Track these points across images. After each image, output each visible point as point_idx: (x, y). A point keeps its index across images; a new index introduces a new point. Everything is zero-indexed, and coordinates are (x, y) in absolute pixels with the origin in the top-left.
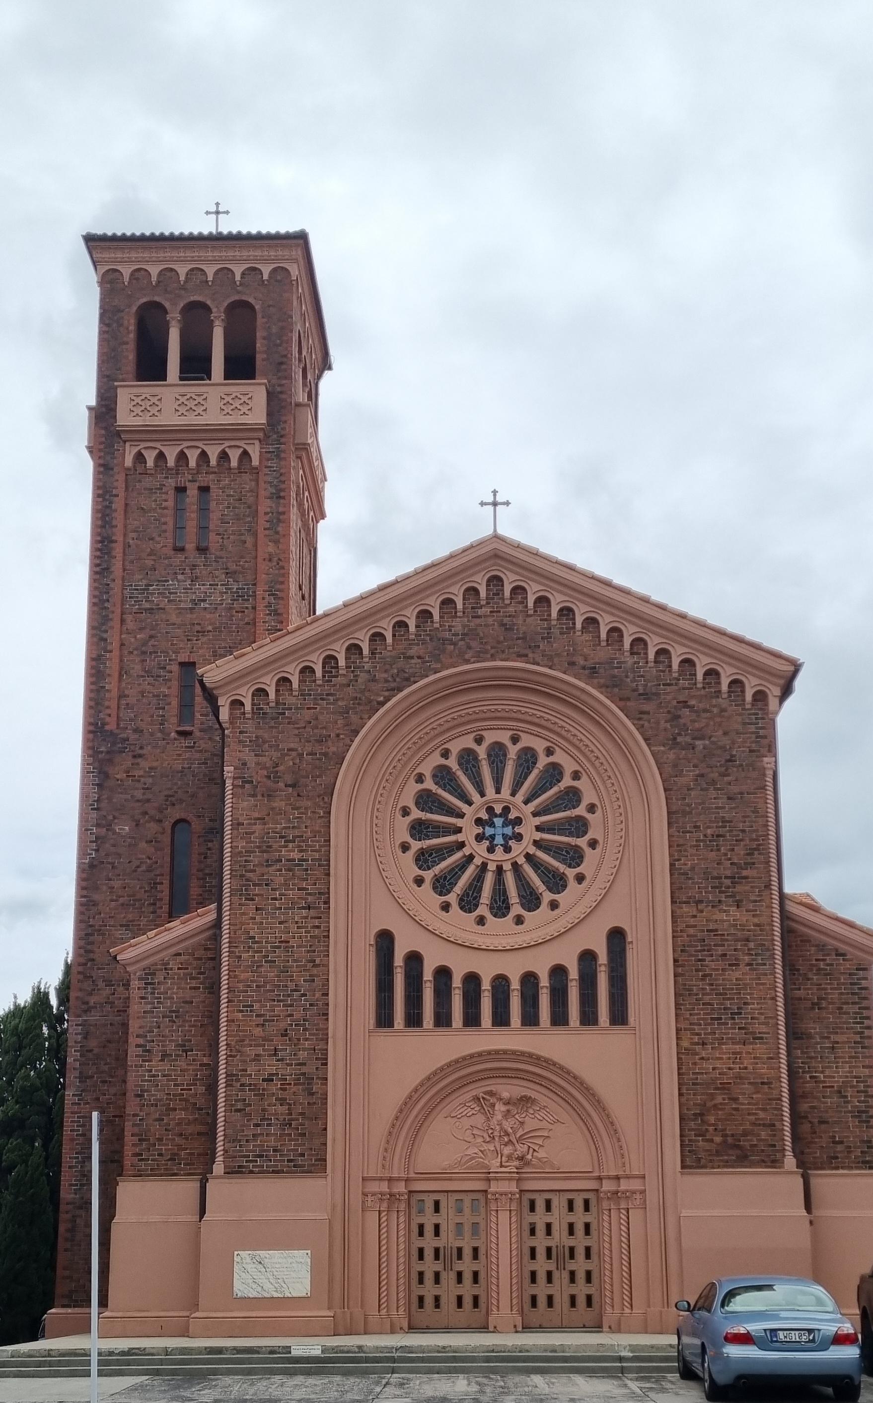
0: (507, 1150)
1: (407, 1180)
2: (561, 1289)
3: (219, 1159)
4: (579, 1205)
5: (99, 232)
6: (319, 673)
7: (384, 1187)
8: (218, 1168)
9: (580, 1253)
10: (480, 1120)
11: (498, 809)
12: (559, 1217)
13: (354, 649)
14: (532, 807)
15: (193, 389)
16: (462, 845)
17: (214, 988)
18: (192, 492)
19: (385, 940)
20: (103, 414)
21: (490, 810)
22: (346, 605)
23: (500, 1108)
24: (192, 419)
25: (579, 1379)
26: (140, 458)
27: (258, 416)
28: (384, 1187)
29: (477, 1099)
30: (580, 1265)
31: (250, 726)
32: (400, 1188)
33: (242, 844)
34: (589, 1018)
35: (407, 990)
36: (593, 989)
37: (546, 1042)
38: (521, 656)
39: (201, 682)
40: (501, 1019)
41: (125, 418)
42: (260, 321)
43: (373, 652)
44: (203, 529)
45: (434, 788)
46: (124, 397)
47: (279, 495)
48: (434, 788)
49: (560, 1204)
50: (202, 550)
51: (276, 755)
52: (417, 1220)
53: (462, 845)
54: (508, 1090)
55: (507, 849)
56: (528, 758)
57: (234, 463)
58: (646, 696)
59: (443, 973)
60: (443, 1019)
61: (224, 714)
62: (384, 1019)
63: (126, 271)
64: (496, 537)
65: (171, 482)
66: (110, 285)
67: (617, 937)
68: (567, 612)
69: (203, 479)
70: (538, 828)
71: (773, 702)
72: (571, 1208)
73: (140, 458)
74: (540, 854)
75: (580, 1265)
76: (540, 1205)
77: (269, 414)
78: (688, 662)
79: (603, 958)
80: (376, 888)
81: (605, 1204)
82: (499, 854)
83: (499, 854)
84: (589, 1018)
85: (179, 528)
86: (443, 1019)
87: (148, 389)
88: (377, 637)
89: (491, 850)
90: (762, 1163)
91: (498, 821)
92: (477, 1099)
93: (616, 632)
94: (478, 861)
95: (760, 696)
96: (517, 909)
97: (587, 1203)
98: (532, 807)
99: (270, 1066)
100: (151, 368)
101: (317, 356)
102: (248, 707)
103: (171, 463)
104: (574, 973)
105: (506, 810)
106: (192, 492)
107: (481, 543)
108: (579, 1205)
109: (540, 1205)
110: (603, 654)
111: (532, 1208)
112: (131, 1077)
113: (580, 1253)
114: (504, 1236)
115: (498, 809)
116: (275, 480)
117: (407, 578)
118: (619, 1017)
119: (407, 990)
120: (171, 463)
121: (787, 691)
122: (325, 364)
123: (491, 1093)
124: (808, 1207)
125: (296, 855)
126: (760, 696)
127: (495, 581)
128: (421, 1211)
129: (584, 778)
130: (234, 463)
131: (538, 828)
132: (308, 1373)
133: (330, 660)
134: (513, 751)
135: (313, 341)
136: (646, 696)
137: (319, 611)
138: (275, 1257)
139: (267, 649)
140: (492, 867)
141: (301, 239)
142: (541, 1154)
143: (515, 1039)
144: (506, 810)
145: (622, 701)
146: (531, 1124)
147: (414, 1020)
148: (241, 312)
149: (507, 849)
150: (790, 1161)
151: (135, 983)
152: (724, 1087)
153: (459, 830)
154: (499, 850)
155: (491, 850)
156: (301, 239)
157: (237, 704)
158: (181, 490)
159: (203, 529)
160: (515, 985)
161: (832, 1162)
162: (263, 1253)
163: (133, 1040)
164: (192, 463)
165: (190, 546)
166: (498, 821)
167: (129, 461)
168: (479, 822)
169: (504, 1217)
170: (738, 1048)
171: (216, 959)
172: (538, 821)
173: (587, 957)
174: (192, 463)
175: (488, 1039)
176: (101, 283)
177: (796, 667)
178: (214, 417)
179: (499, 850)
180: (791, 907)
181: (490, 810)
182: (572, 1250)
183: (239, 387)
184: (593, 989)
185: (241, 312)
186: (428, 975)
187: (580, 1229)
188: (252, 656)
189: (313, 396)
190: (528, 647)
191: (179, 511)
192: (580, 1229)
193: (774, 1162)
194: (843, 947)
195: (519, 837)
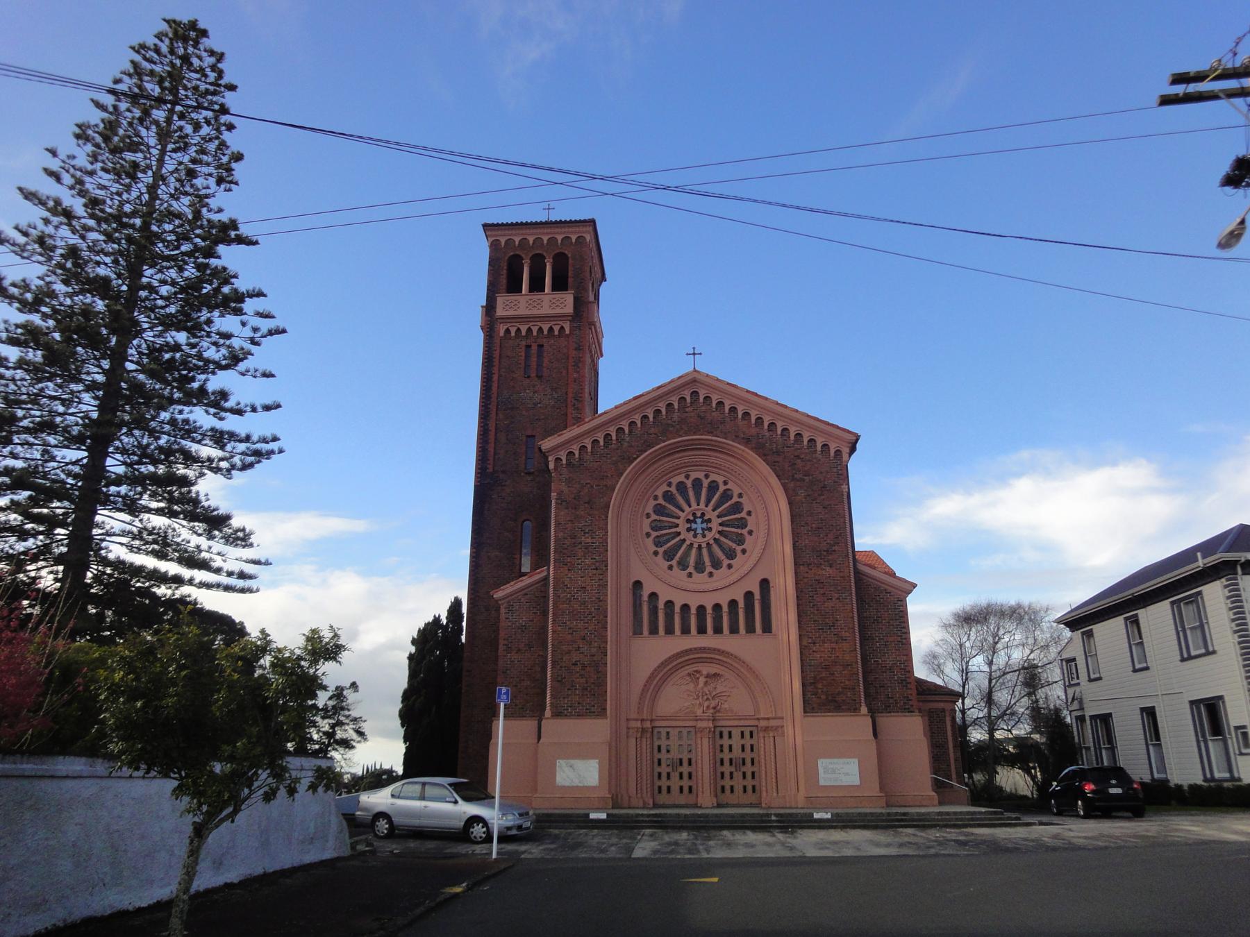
0: (706, 704)
1: (652, 720)
2: (738, 782)
3: (548, 708)
4: (747, 734)
5: (490, 222)
6: (602, 443)
7: (639, 724)
8: (548, 713)
9: (748, 761)
10: (691, 686)
11: (699, 514)
12: (736, 742)
13: (620, 430)
14: (716, 513)
15: (536, 296)
16: (679, 534)
17: (545, 613)
18: (534, 347)
19: (638, 585)
20: (490, 309)
21: (694, 514)
22: (616, 407)
23: (702, 680)
24: (535, 312)
25: (749, 833)
26: (508, 331)
27: (569, 309)
28: (639, 724)
29: (689, 675)
30: (748, 769)
31: (565, 471)
32: (648, 725)
33: (561, 535)
34: (750, 629)
35: (652, 615)
36: (753, 611)
37: (726, 642)
38: (710, 433)
39: (540, 449)
40: (702, 630)
41: (500, 312)
42: (570, 261)
43: (630, 431)
44: (539, 365)
45: (664, 503)
46: (501, 300)
47: (579, 349)
48: (664, 503)
49: (736, 733)
50: (539, 377)
51: (578, 486)
52: (656, 743)
53: (679, 534)
54: (706, 669)
55: (704, 536)
56: (713, 487)
57: (556, 333)
58: (778, 453)
59: (670, 604)
60: (669, 631)
61: (551, 466)
62: (637, 631)
63: (503, 241)
64: (695, 370)
65: (524, 343)
66: (494, 246)
67: (765, 584)
68: (733, 409)
69: (540, 341)
70: (721, 524)
71: (845, 456)
72: (742, 737)
73: (508, 331)
74: (723, 539)
75: (748, 769)
76: (726, 735)
77: (575, 308)
78: (799, 435)
79: (757, 596)
80: (635, 560)
81: (761, 735)
82: (700, 539)
83: (700, 539)
84: (750, 629)
85: (527, 366)
86: (669, 631)
87: (513, 297)
88: (632, 424)
89: (695, 536)
90: (849, 710)
91: (699, 521)
92: (689, 675)
93: (759, 419)
94: (688, 542)
95: (838, 453)
96: (709, 569)
97: (751, 733)
98: (716, 513)
99: (575, 657)
100: (514, 286)
101: (599, 275)
102: (564, 462)
103: (524, 333)
104: (741, 604)
105: (703, 514)
106: (534, 347)
107: (687, 375)
108: (747, 734)
109: (726, 735)
110: (754, 431)
111: (721, 736)
112: (501, 662)
113: (748, 761)
114: (704, 751)
115: (699, 514)
116: (579, 340)
117: (648, 393)
118: (767, 628)
119: (652, 615)
120: (524, 333)
121: (853, 449)
122: (603, 278)
123: (697, 672)
124: (875, 734)
125: (589, 540)
126: (838, 453)
127: (695, 394)
128: (659, 738)
129: (745, 497)
130: (556, 333)
131: (721, 524)
132: (597, 828)
133: (608, 436)
134: (706, 483)
135: (597, 268)
136: (778, 453)
137: (600, 412)
138: (579, 764)
139: (576, 431)
140: (696, 545)
141: (592, 222)
142: (726, 706)
143: (709, 641)
144: (703, 514)
145: (764, 456)
146: (720, 688)
147: (654, 631)
148: (561, 262)
149: (704, 536)
150: (864, 709)
151: (503, 611)
152: (827, 668)
153: (677, 526)
154: (699, 536)
155: (695, 536)
156: (592, 222)
157: (558, 460)
158: (528, 347)
159: (539, 365)
160: (709, 610)
161: (888, 709)
162: (572, 762)
163: (501, 642)
164: (535, 333)
165: (533, 375)
166: (699, 521)
167: (502, 334)
168: (688, 521)
169: (706, 741)
170: (834, 645)
171: (546, 597)
172: (720, 520)
173: (749, 595)
174: (535, 333)
175: (695, 641)
176: (491, 247)
177: (858, 438)
178: (546, 310)
179: (699, 536)
180: (861, 567)
181: (694, 514)
182: (744, 760)
183: (559, 295)
184: (753, 611)
185: (561, 262)
186: (661, 605)
187: (748, 748)
188: (567, 435)
189: (597, 297)
190: (713, 427)
191: (527, 356)
192: (748, 748)
193: (856, 710)
194: (890, 589)
195: (710, 529)
